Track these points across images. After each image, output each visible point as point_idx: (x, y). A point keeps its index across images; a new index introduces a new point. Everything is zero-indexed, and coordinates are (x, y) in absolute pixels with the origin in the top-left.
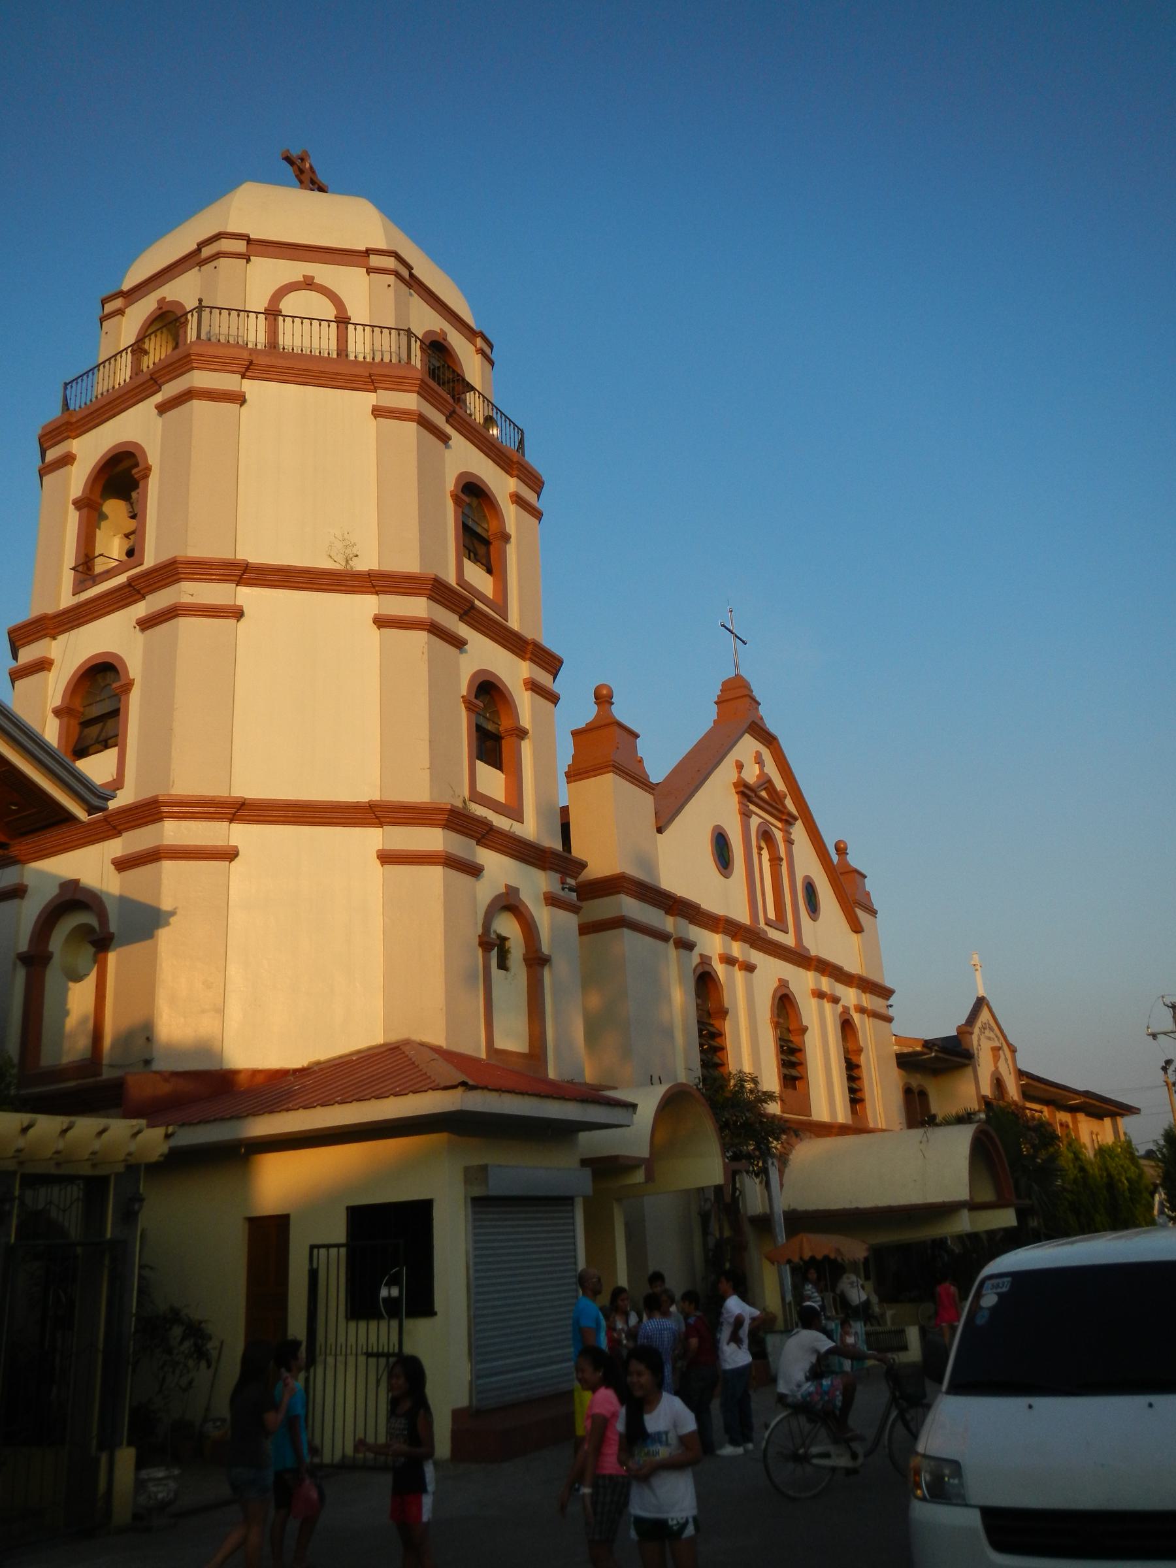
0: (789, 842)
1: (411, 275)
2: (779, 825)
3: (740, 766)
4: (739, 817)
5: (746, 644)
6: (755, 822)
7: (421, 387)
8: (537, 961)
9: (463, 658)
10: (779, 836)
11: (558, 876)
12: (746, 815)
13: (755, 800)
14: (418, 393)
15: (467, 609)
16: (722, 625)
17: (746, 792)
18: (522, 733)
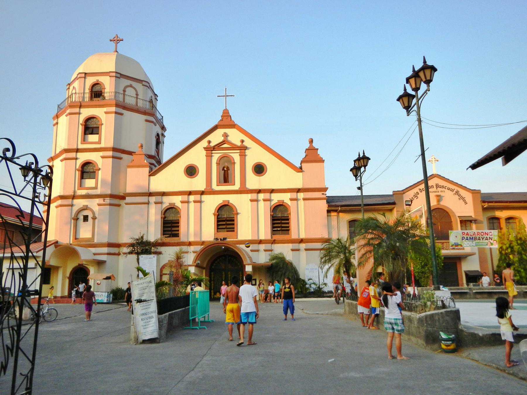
0: (243, 156)
1: (85, 74)
2: (239, 151)
3: (209, 142)
4: (205, 158)
5: (234, 96)
6: (216, 156)
7: (69, 107)
8: (94, 218)
9: (78, 161)
10: (236, 156)
11: (102, 199)
12: (209, 157)
13: (215, 149)
14: (70, 108)
15: (77, 150)
16: (218, 97)
17: (210, 150)
18: (99, 169)
